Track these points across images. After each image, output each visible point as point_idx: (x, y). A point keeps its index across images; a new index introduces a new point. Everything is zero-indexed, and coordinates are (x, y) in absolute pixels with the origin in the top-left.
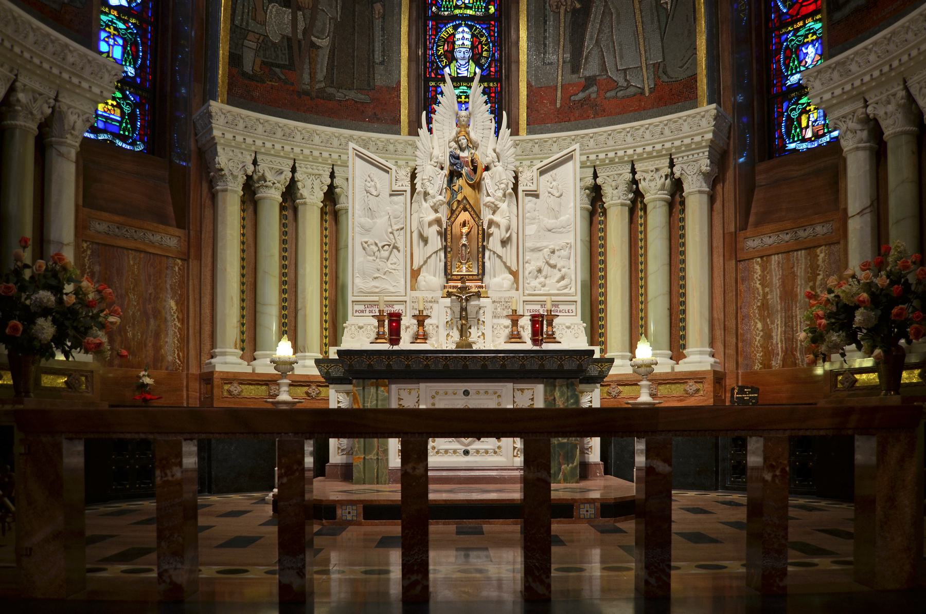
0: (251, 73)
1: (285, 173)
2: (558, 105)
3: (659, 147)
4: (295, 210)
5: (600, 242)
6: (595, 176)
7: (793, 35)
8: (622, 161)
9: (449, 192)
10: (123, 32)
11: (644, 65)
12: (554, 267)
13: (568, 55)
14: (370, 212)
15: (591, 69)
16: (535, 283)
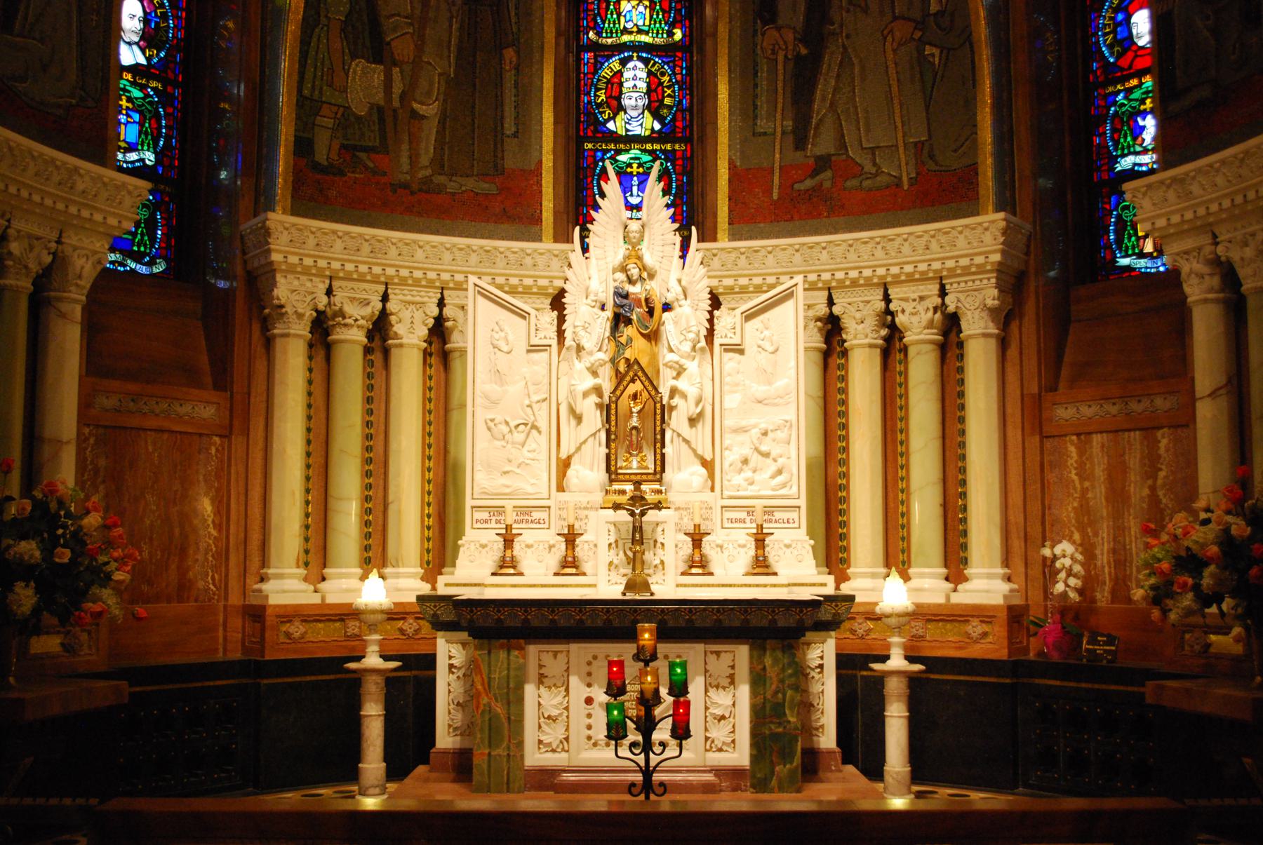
0: (326, 163)
1: (372, 304)
2: (775, 196)
3: (922, 267)
4: (386, 353)
5: (839, 397)
6: (831, 303)
7: (1126, 98)
8: (869, 283)
9: (613, 344)
10: (139, 102)
11: (901, 143)
12: (766, 455)
13: (789, 124)
16: (738, 479)
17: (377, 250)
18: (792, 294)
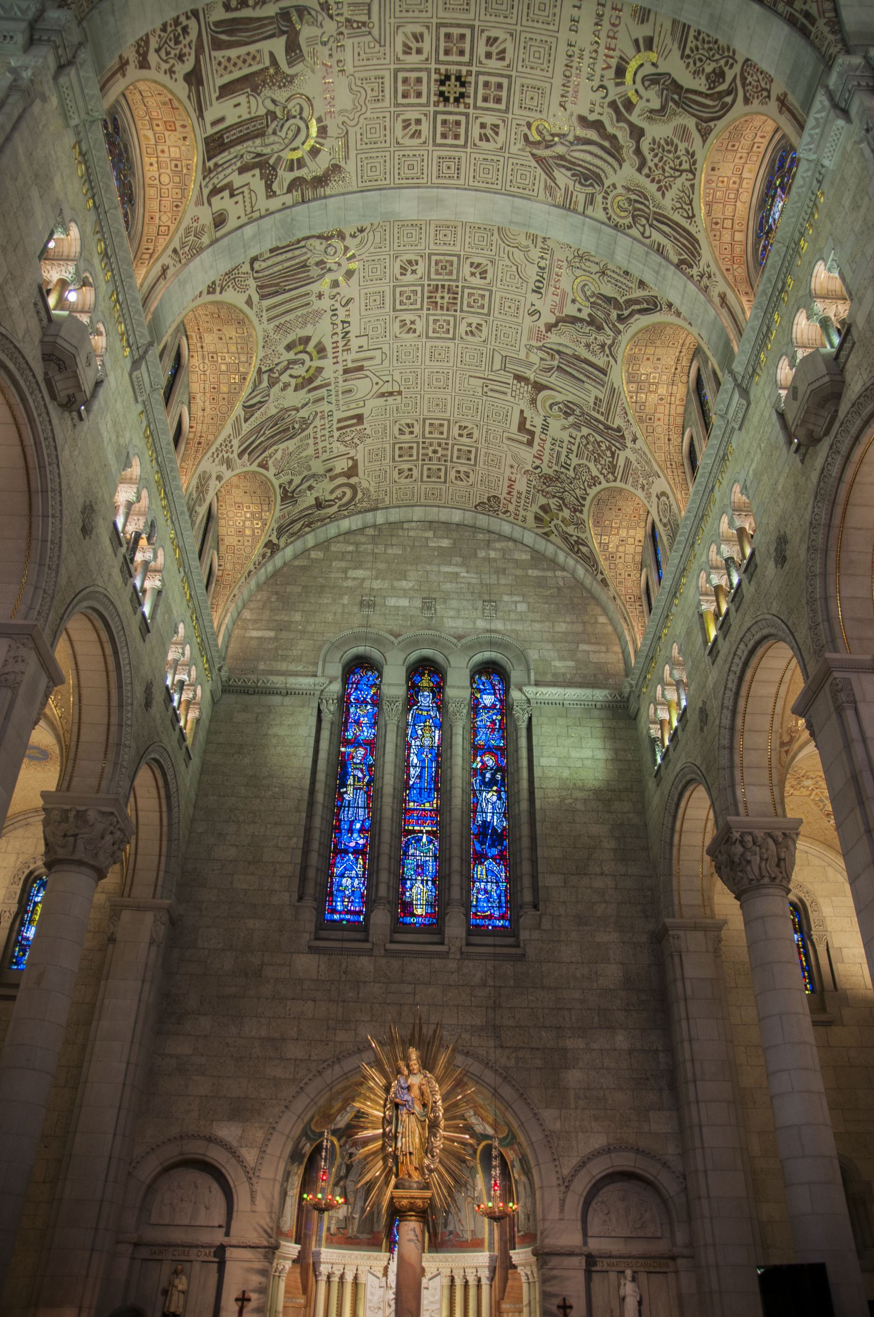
14: (372, 1294)
17: (344, 1256)
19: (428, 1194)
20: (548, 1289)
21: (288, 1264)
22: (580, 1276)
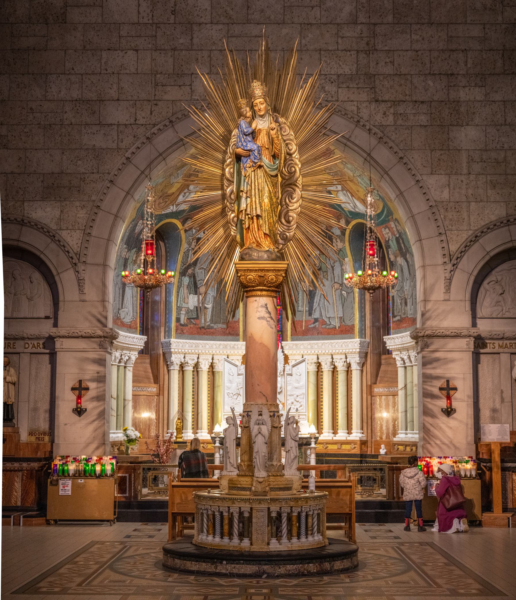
2: (303, 329)
3: (341, 351)
6: (318, 359)
8: (327, 354)
12: (298, 402)
13: (307, 308)
15: (316, 315)
17: (197, 346)
18: (304, 361)
19: (282, 265)
20: (429, 372)
21: (134, 355)
22: (467, 359)
